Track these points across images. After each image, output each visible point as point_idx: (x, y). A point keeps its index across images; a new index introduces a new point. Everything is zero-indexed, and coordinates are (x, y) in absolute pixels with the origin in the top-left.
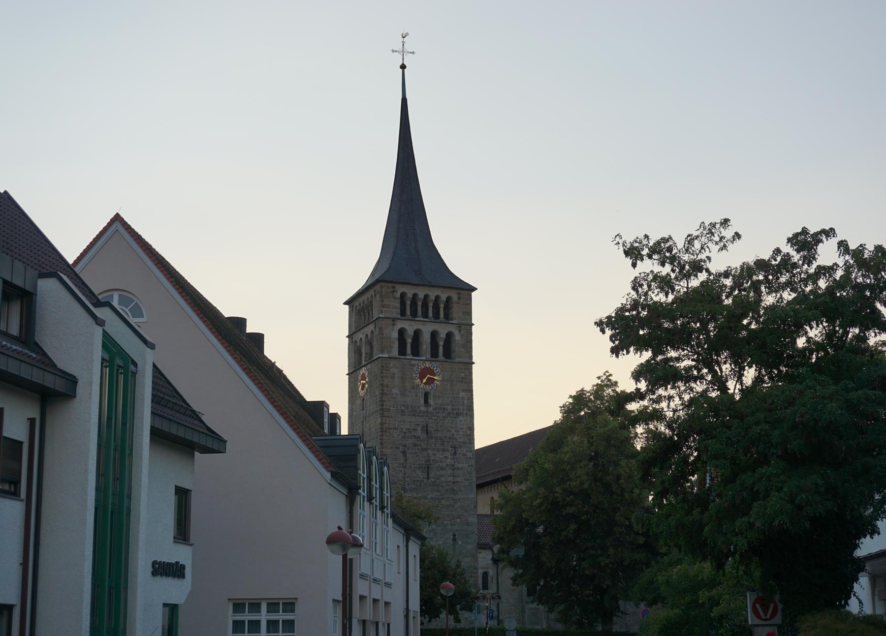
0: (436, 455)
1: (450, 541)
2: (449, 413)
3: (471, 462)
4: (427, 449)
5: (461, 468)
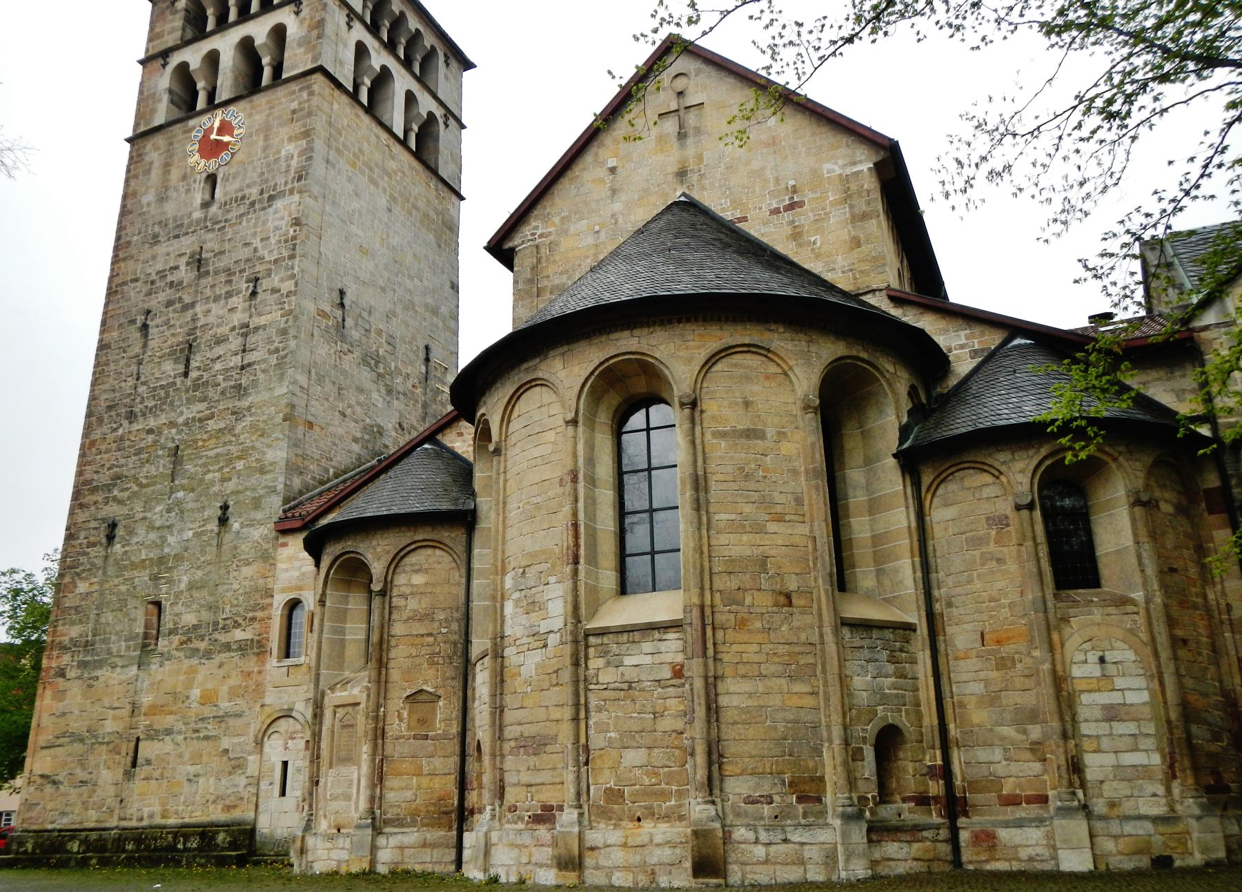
0: (209, 311)
1: (213, 526)
2: (253, 204)
3: (290, 304)
4: (193, 305)
5: (264, 327)
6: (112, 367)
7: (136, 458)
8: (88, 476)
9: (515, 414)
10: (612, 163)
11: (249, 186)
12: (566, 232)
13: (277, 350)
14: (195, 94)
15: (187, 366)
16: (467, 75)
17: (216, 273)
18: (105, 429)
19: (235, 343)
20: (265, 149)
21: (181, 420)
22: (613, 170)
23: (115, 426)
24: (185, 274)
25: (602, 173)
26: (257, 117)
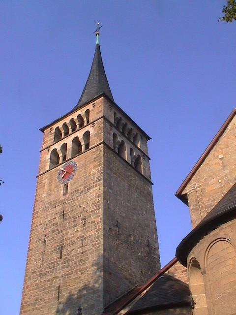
2: (82, 192)
3: (99, 226)
4: (62, 231)
5: (89, 237)
6: (33, 257)
7: (43, 292)
8: (26, 300)
9: (210, 255)
10: (221, 156)
11: (80, 186)
12: (208, 184)
13: (95, 245)
14: (58, 158)
15: (61, 254)
16: (149, 142)
17: (70, 218)
18: (32, 281)
19: (79, 243)
20: (85, 172)
21: (60, 275)
22: (222, 159)
23: (35, 280)
24: (58, 220)
25: (218, 161)
26: (81, 162)
